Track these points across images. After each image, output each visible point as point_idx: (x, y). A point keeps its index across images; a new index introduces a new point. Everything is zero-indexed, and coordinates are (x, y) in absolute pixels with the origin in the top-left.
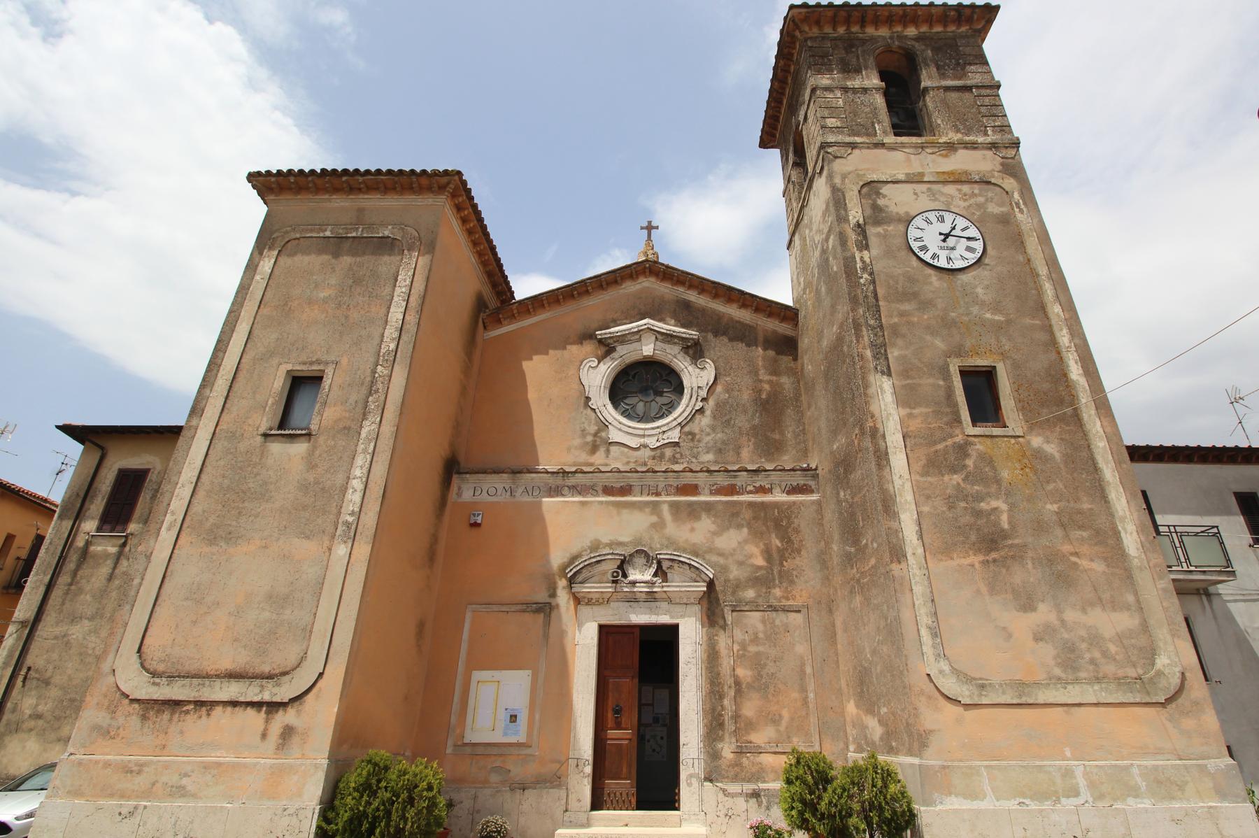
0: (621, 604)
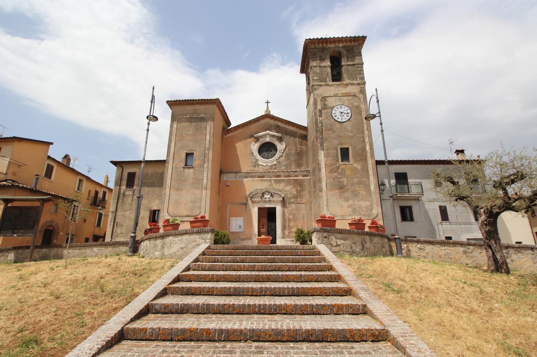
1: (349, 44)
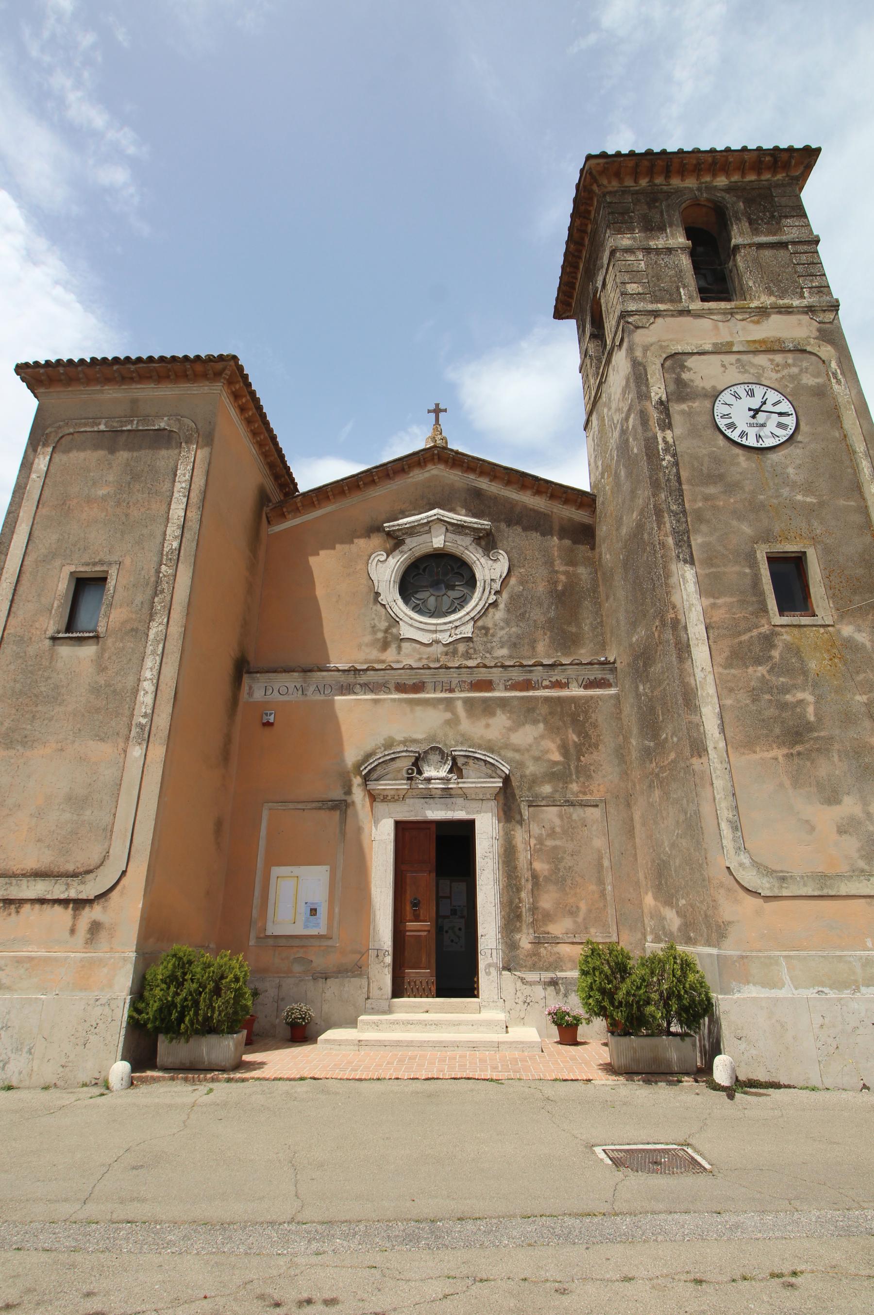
0: (417, 800)
1: (751, 177)
